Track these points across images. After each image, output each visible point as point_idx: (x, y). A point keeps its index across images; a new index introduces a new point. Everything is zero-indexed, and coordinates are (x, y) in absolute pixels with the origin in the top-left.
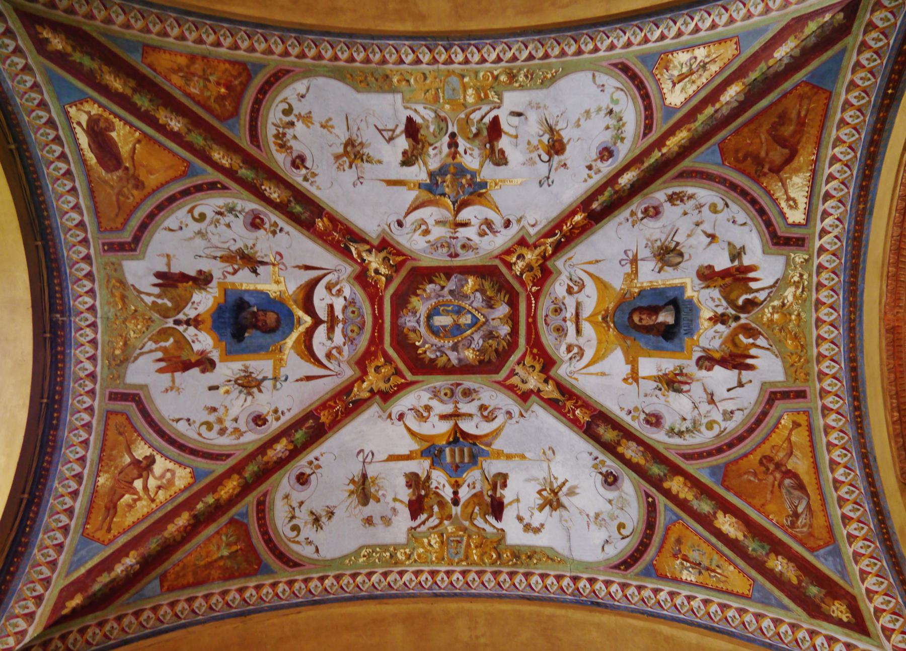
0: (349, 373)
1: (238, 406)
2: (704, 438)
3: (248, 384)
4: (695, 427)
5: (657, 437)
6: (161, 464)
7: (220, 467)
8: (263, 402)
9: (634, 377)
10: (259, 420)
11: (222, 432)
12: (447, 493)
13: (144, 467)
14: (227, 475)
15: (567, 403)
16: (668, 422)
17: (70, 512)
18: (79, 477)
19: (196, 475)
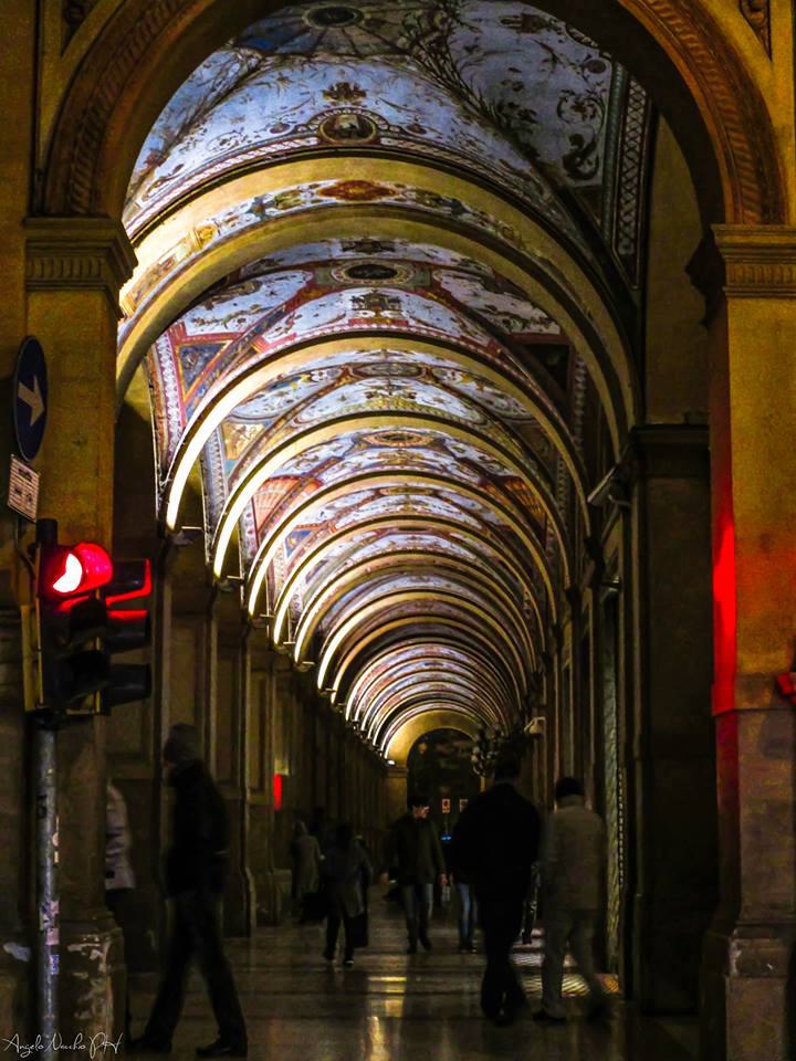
0: (332, 382)
1: (278, 400)
2: (512, 413)
3: (281, 394)
4: (508, 409)
5: (491, 407)
6: (248, 427)
7: (274, 420)
8: (289, 397)
9: (481, 389)
10: (289, 402)
11: (273, 409)
12: (387, 393)
13: (244, 429)
14: (280, 420)
15: (447, 388)
16: (496, 403)
17: (219, 456)
18: (217, 445)
19: (266, 425)
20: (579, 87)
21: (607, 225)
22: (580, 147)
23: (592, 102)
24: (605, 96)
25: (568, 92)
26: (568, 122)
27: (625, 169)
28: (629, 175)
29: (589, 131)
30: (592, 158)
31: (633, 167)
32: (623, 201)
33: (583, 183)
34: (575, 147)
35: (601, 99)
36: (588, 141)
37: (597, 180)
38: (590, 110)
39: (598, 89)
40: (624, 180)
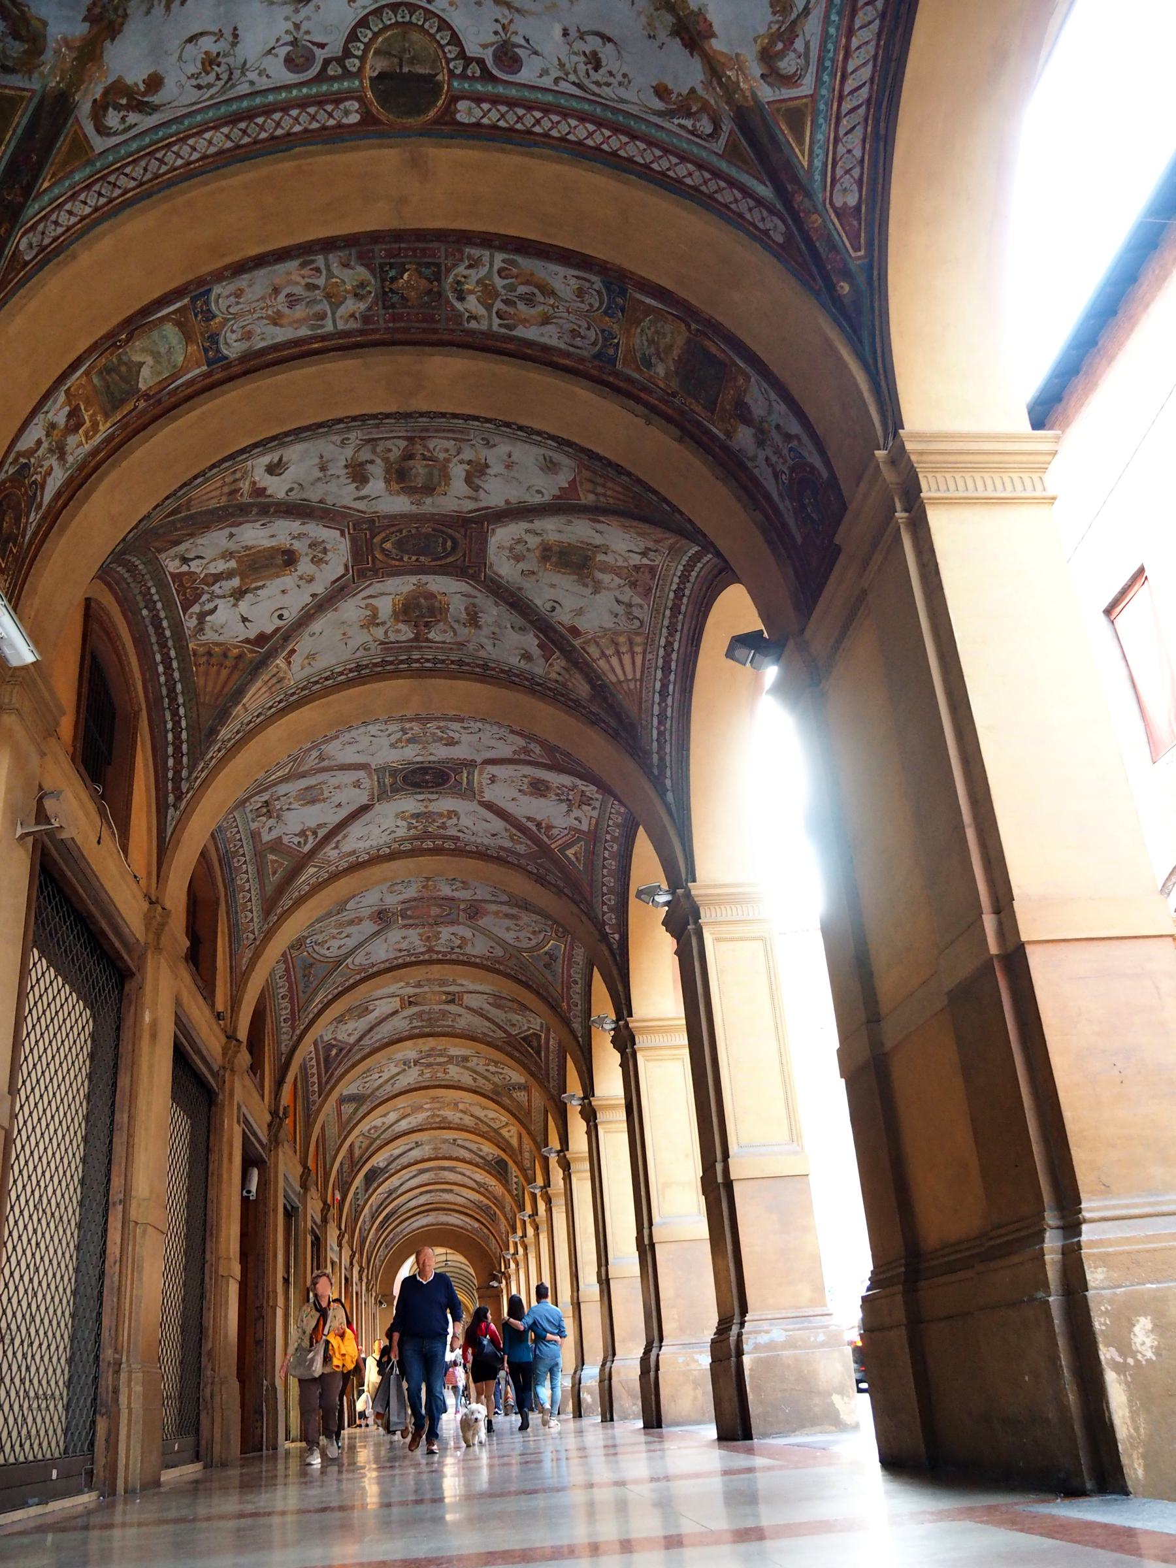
20: (251, 47)
21: (46, 198)
22: (144, 94)
23: (225, 76)
24: (244, 89)
25: (236, 36)
26: (180, 58)
27: (128, 170)
28: (123, 182)
29: (176, 90)
30: (133, 118)
31: (134, 179)
32: (82, 197)
33: (89, 129)
34: (142, 87)
35: (233, 86)
36: (156, 99)
37: (99, 144)
38: (211, 78)
39: (252, 76)
40: (112, 179)
